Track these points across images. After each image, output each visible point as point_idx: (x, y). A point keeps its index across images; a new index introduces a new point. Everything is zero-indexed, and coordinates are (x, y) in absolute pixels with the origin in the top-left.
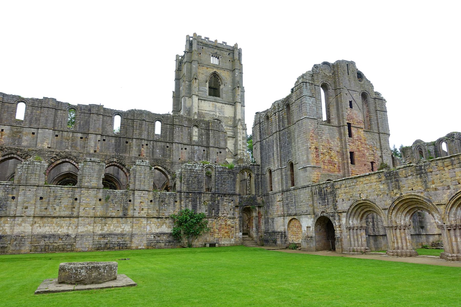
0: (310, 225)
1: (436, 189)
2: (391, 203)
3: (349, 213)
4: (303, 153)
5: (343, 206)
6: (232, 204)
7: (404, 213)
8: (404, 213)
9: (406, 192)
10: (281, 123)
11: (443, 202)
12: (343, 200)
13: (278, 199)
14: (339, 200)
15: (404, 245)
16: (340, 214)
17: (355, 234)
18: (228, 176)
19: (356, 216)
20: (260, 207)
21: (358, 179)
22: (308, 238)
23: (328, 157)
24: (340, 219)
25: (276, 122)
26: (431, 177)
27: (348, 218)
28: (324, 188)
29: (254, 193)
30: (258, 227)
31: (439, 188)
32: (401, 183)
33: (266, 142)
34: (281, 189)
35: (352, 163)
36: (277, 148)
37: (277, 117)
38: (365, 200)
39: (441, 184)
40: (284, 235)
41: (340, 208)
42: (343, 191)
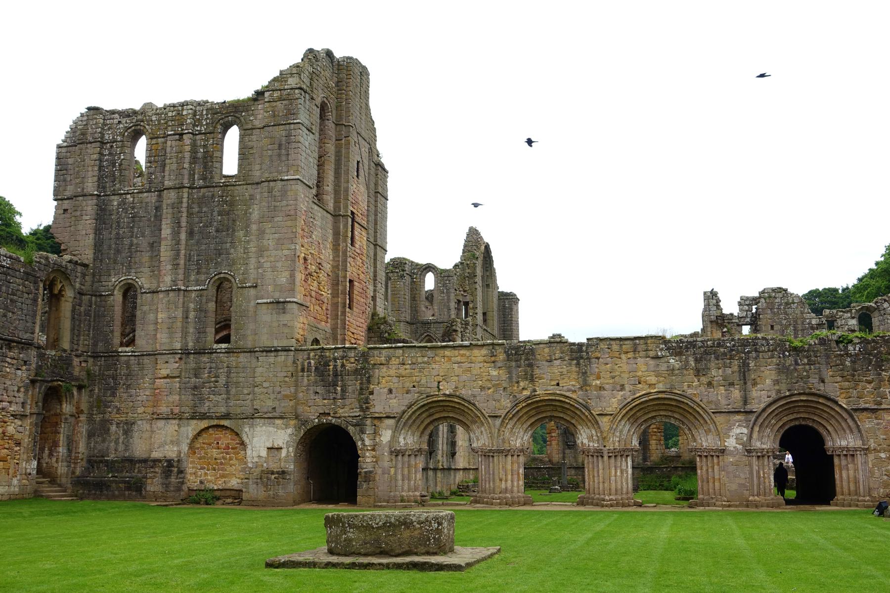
0: (279, 443)
1: (601, 388)
2: (509, 405)
3: (403, 420)
4: (279, 264)
6: (22, 374)
7: (525, 426)
8: (525, 426)
10: (198, 168)
11: (609, 410)
12: (390, 391)
13: (164, 372)
14: (379, 390)
15: (515, 484)
16: (376, 422)
18: (24, 286)
19: (414, 427)
20: (80, 388)
21: (441, 352)
22: (271, 477)
24: (376, 433)
25: (180, 161)
26: (595, 367)
27: (396, 430)
28: (335, 359)
29: (66, 345)
30: (71, 444)
31: (607, 386)
32: (537, 371)
33: (123, 203)
34: (178, 346)
36: (176, 233)
37: (188, 148)
38: (449, 396)
39: (611, 381)
40: (171, 467)
41: (379, 406)
42: (392, 372)
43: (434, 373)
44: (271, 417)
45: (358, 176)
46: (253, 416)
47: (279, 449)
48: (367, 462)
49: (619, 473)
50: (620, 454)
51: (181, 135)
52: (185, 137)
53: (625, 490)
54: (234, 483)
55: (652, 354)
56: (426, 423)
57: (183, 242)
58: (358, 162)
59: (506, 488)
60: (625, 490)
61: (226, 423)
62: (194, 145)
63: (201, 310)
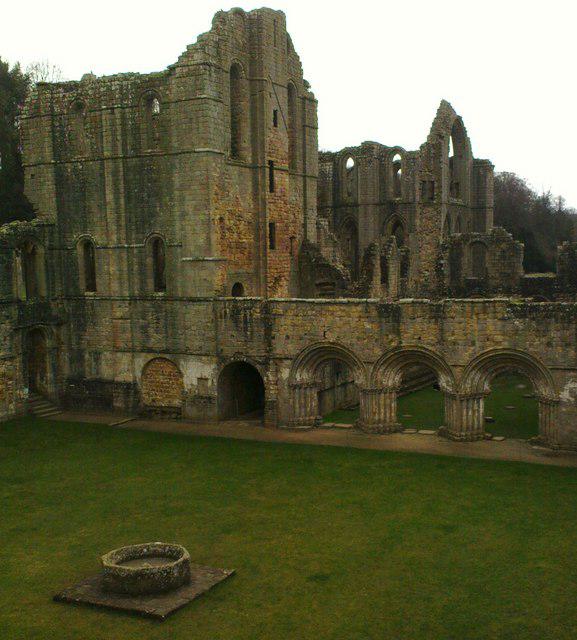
1: (454, 343)
2: (381, 353)
5: (284, 346)
8: (399, 367)
9: (407, 342)
10: (130, 140)
11: (461, 362)
12: (288, 337)
15: (388, 415)
16: (277, 361)
17: (303, 396)
20: (59, 325)
21: (326, 307)
23: (235, 235)
24: (277, 371)
25: (114, 134)
27: (293, 370)
30: (56, 369)
31: (460, 342)
32: (402, 327)
33: (75, 170)
34: (127, 293)
35: (272, 247)
36: (117, 199)
37: (118, 122)
38: (333, 343)
40: (130, 388)
41: (279, 348)
43: (321, 324)
44: (200, 354)
45: (275, 125)
46: (187, 353)
47: (207, 379)
48: (271, 392)
49: (470, 413)
50: (475, 396)
51: (113, 109)
52: (115, 111)
53: (476, 426)
54: (177, 402)
55: (499, 316)
56: (318, 362)
57: (123, 206)
58: (275, 112)
59: (380, 419)
60: (476, 426)
61: (167, 356)
62: (123, 118)
63: (142, 264)
